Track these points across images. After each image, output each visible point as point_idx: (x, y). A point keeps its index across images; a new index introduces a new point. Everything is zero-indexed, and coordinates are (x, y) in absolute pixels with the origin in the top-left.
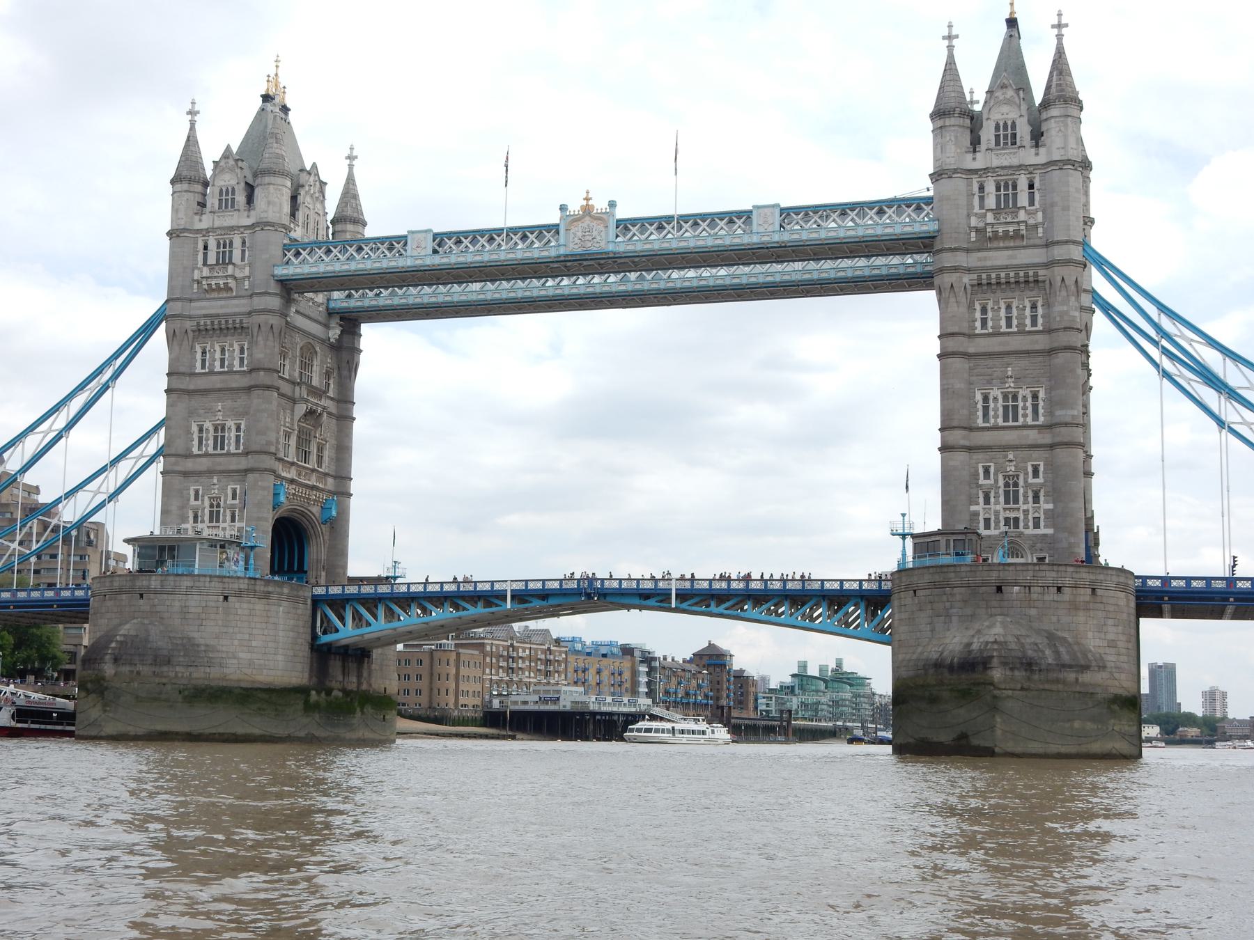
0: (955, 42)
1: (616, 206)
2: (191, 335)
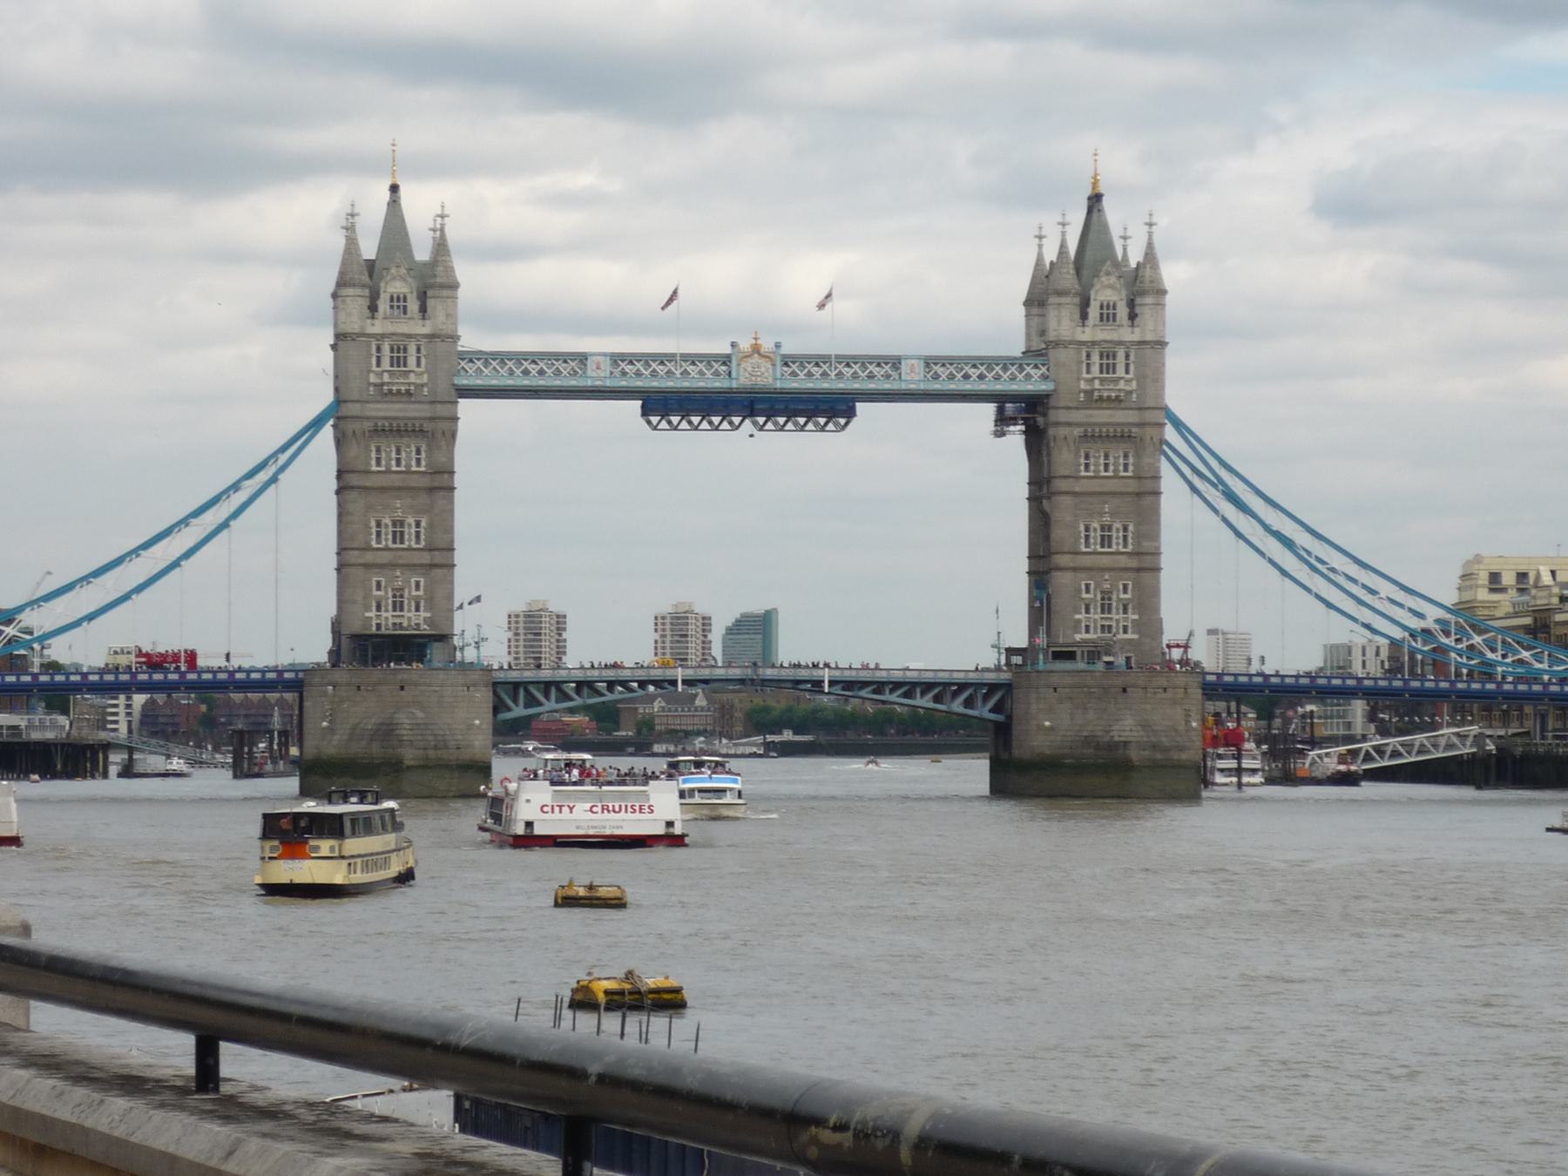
1: (780, 346)
2: (367, 434)
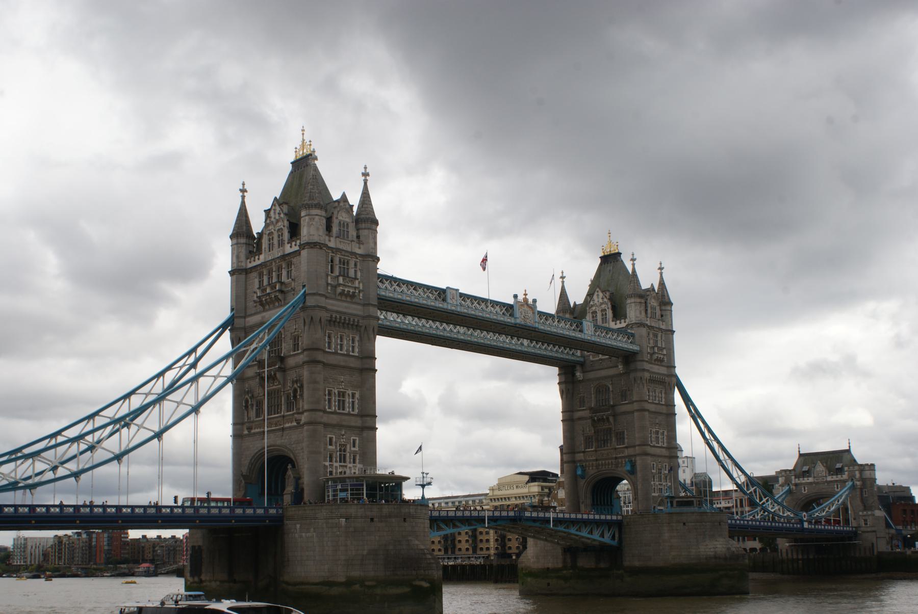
0: (635, 262)
